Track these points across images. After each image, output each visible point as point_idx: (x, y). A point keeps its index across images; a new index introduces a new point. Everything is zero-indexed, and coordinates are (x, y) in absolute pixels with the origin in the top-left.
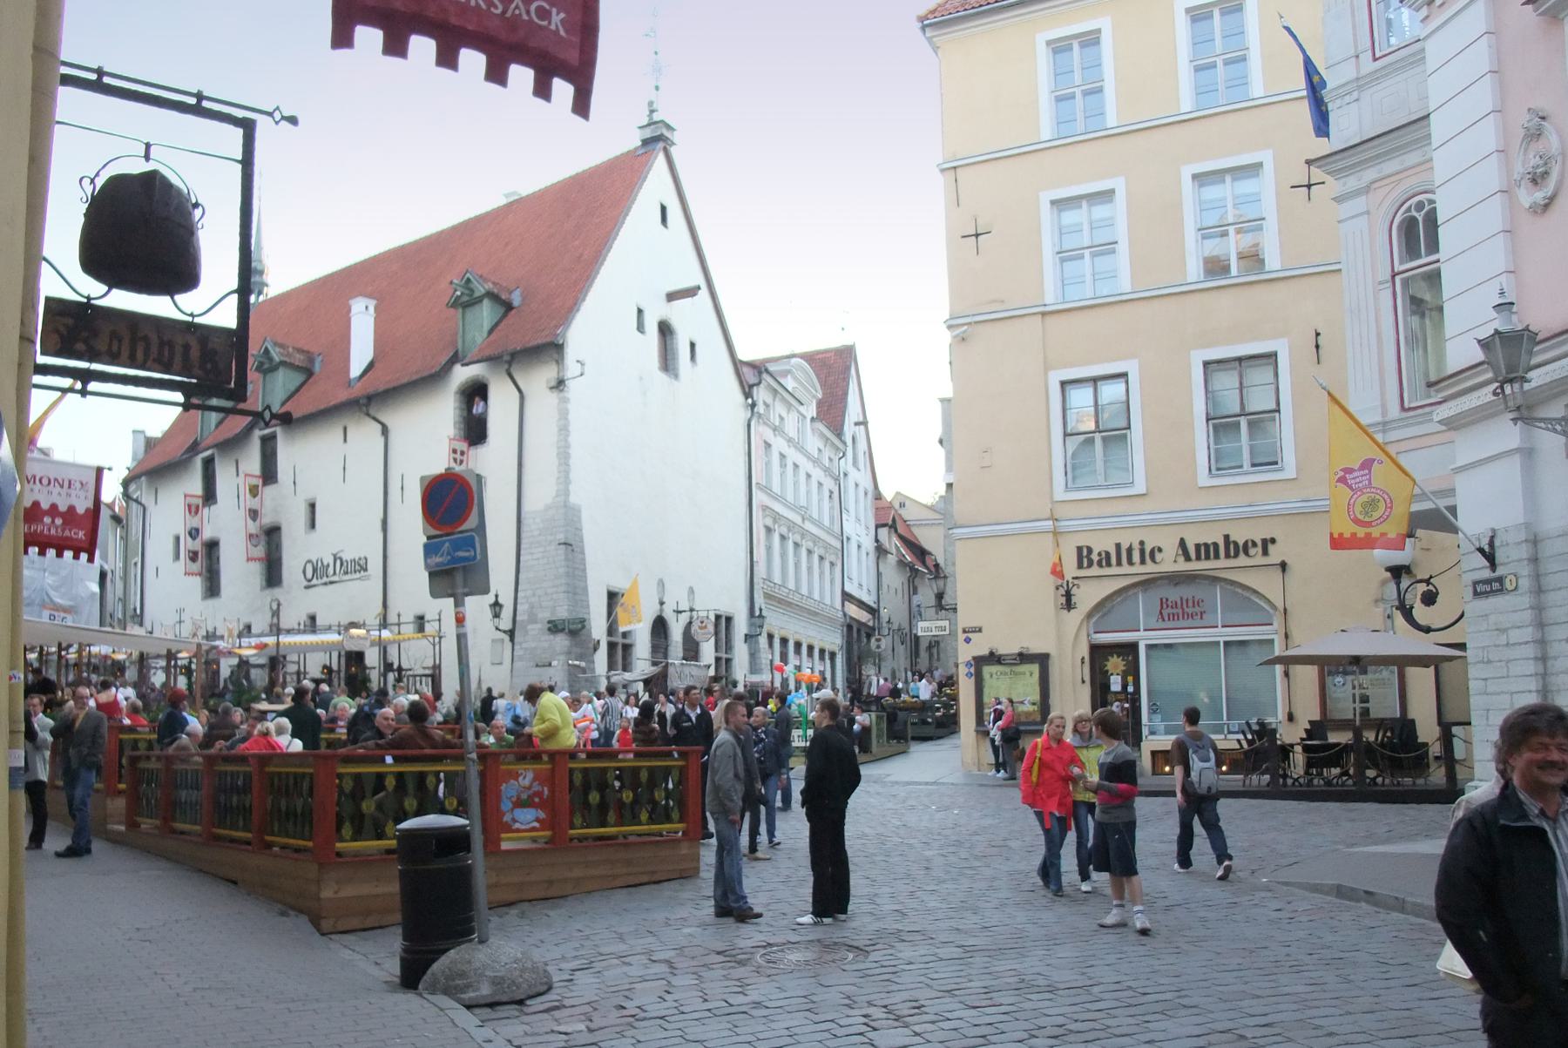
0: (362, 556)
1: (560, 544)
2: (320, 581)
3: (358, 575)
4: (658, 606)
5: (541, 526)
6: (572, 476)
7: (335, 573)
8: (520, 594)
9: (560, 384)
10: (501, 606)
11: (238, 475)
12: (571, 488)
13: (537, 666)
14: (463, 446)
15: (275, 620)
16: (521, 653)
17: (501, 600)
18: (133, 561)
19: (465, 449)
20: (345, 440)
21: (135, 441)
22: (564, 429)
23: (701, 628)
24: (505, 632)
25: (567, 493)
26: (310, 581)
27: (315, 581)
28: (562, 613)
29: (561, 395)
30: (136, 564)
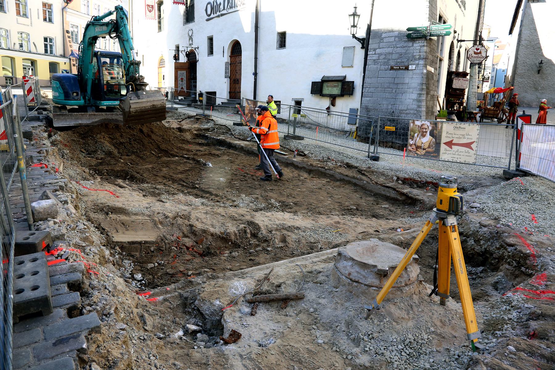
2: (215, 15)
7: (224, 9)
13: (392, 68)
15: (191, 42)
16: (375, 57)
23: (475, 53)
24: (358, 39)
27: (212, 16)
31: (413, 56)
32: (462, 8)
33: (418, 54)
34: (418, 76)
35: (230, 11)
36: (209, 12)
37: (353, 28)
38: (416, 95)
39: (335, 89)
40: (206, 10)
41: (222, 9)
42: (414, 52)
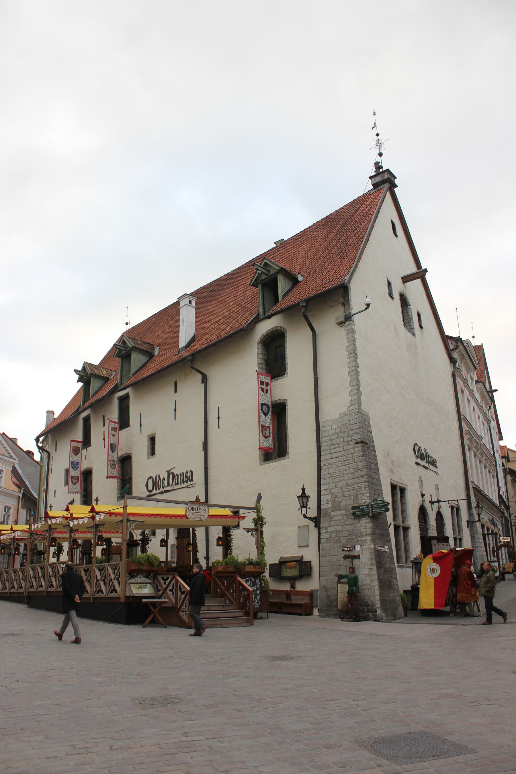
0: (189, 470)
1: (356, 443)
2: (158, 491)
3: (186, 485)
4: (420, 498)
5: (338, 431)
6: (361, 389)
7: (168, 485)
8: (322, 487)
9: (348, 318)
10: (308, 497)
11: (104, 425)
12: (362, 398)
14: (266, 379)
16: (327, 536)
17: (307, 493)
18: (43, 489)
19: (269, 381)
20: (176, 391)
21: (48, 417)
22: (353, 354)
24: (310, 519)
25: (360, 404)
26: (151, 491)
27: (154, 492)
28: (365, 499)
29: (349, 327)
30: (44, 490)
31: (361, 533)
32: (431, 467)
33: (364, 530)
34: (367, 552)
35: (176, 487)
36: (150, 488)
37: (303, 509)
38: (368, 570)
39: (293, 570)
40: (147, 485)
41: (166, 484)
42: (361, 529)
